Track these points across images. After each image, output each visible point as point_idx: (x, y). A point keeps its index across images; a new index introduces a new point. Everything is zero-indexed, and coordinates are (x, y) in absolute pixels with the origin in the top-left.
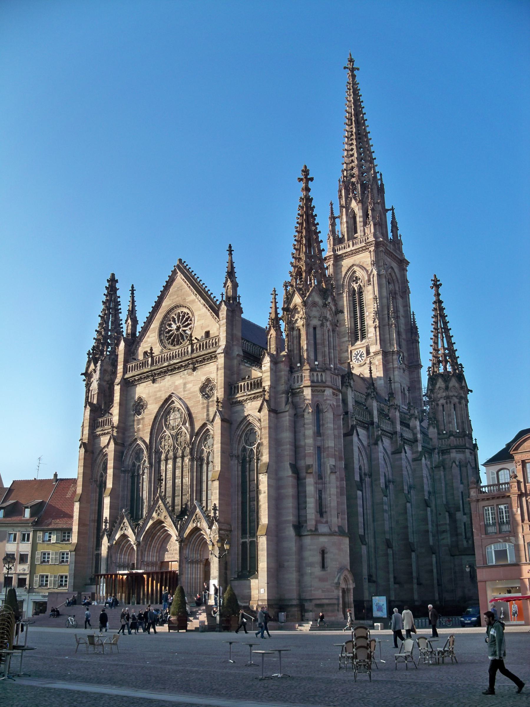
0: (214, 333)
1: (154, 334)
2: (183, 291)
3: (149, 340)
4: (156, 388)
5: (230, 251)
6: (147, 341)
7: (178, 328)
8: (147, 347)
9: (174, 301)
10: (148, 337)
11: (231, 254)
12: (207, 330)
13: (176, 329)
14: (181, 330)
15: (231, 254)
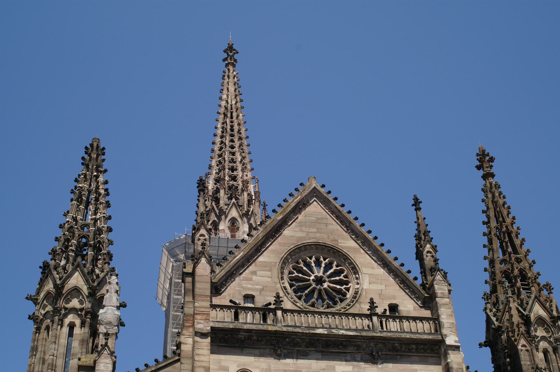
0: (408, 311)
1: (268, 273)
2: (330, 227)
3: (254, 278)
4: (288, 364)
5: (417, 204)
6: (251, 279)
7: (320, 281)
8: (249, 289)
9: (311, 235)
10: (254, 273)
11: (418, 209)
12: (394, 302)
13: (313, 280)
14: (325, 285)
15: (418, 209)
